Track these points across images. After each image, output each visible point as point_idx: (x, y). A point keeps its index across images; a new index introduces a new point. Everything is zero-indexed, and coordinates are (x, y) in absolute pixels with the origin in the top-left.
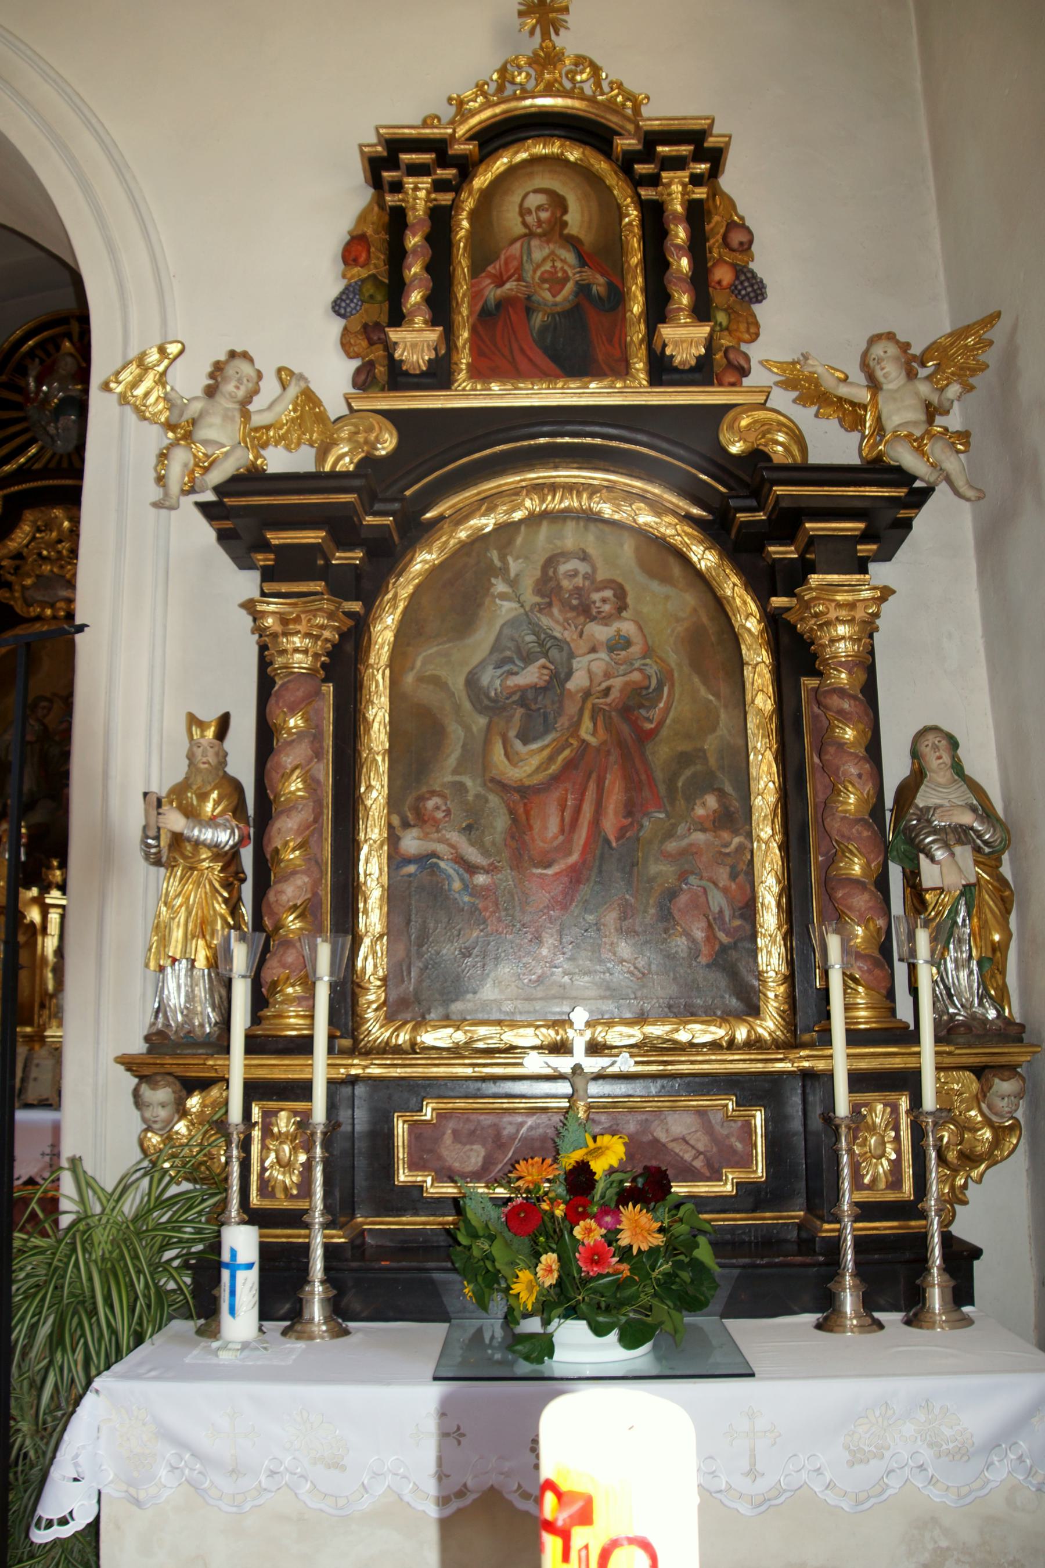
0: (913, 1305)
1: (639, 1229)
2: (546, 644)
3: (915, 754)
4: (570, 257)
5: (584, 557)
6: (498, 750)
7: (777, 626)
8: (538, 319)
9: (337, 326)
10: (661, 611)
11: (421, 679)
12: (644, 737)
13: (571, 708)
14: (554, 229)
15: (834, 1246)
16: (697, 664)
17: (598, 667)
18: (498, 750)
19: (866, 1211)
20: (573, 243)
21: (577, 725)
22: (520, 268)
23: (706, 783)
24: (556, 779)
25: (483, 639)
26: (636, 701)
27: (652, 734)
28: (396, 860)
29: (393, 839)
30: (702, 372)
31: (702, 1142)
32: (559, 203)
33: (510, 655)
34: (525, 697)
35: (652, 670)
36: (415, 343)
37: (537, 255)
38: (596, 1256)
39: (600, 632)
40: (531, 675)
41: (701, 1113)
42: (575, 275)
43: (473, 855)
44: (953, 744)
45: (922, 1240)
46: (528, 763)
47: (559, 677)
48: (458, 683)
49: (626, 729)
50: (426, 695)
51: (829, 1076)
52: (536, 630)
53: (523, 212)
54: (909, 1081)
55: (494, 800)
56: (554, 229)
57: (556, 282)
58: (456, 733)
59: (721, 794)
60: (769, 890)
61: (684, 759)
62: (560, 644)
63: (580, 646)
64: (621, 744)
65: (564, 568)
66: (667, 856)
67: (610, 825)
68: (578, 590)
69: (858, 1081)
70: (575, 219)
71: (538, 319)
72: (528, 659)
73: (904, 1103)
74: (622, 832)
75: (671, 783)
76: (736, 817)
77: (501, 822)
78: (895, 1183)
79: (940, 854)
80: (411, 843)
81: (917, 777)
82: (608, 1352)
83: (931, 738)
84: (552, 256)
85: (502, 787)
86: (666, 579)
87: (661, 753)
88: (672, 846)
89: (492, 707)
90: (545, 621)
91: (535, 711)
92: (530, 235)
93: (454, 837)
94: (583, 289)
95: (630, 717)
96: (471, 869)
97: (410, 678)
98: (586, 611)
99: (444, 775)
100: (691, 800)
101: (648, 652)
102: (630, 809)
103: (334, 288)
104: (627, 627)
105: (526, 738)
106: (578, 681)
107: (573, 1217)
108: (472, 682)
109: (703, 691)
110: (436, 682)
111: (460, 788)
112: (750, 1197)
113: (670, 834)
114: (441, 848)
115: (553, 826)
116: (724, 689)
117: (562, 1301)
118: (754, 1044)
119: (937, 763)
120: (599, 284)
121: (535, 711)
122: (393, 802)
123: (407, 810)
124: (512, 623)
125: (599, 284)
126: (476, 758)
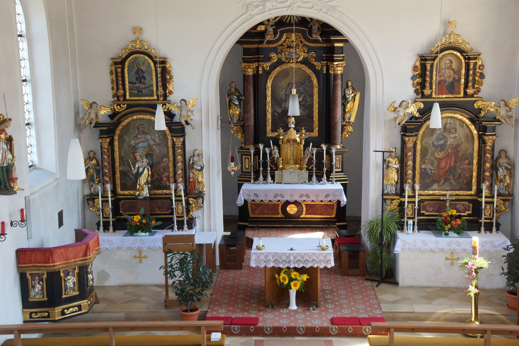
0: (491, 231)
1: (459, 222)
2: (444, 137)
3: (500, 154)
4: (452, 72)
5: (451, 124)
6: (436, 154)
7: (480, 137)
8: (446, 84)
9: (411, 82)
10: (461, 133)
11: (425, 143)
12: (458, 151)
13: (447, 147)
14: (450, 68)
15: (481, 223)
16: (467, 141)
17: (452, 141)
18: (436, 154)
19: (485, 219)
20: (453, 69)
21: (448, 150)
22: (444, 75)
23: (467, 158)
24: (445, 157)
25: (435, 137)
26: (458, 146)
27: (459, 151)
28: (421, 169)
29: (421, 166)
30: (472, 96)
31: (463, 208)
32: (451, 62)
33: (438, 140)
34: (441, 146)
35: (460, 141)
36: (427, 92)
37: (447, 72)
38: (455, 225)
39: (452, 136)
40: (441, 142)
41: (463, 204)
42: (453, 76)
43: (432, 168)
44: (506, 152)
45: (493, 223)
46: (440, 155)
47: (446, 142)
48: (431, 143)
49: (455, 150)
50: (426, 145)
51: (482, 202)
52: (443, 135)
53: (445, 64)
54: (492, 203)
55: (435, 160)
56: (450, 68)
57: (450, 77)
58: (430, 151)
59: (469, 160)
60: (475, 174)
61: (464, 155)
62: (446, 137)
63: (449, 138)
64: (454, 152)
65: (448, 126)
66: (460, 169)
67: (452, 164)
68: (449, 129)
69: (486, 203)
70: (454, 66)
71: (446, 84)
72: (441, 140)
73: (492, 206)
74: (454, 165)
75: (461, 158)
76: (471, 163)
77: (436, 164)
78: (490, 215)
79: (501, 170)
80: (423, 166)
81: (499, 157)
82: (456, 235)
83: (502, 152)
84: (449, 72)
85: (436, 158)
86: (463, 127)
87: (460, 154)
88: (461, 167)
89: (436, 147)
90: (444, 134)
91: (442, 148)
92: (446, 68)
93: (430, 166)
94: (454, 78)
95: (456, 148)
96: (431, 170)
97: (423, 143)
98: (450, 132)
99: (428, 157)
100: (464, 161)
101: (459, 139)
102: (455, 162)
103: (411, 74)
104: (457, 135)
105: (440, 152)
106: (449, 143)
107: (451, 220)
108: (433, 143)
109: (467, 145)
110: (428, 143)
111: (430, 159)
112: (469, 215)
113: (461, 166)
114: (427, 167)
115: (444, 164)
116: (471, 144)
117: (450, 230)
118: (471, 195)
119: (503, 155)
120: (457, 77)
121: (442, 148)
122: (421, 161)
123: (423, 161)
124: (439, 134)
125: (457, 77)
126: (433, 154)
